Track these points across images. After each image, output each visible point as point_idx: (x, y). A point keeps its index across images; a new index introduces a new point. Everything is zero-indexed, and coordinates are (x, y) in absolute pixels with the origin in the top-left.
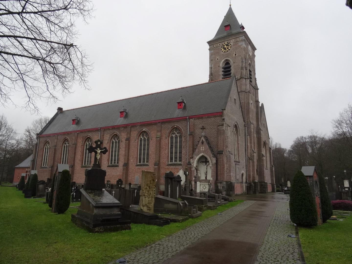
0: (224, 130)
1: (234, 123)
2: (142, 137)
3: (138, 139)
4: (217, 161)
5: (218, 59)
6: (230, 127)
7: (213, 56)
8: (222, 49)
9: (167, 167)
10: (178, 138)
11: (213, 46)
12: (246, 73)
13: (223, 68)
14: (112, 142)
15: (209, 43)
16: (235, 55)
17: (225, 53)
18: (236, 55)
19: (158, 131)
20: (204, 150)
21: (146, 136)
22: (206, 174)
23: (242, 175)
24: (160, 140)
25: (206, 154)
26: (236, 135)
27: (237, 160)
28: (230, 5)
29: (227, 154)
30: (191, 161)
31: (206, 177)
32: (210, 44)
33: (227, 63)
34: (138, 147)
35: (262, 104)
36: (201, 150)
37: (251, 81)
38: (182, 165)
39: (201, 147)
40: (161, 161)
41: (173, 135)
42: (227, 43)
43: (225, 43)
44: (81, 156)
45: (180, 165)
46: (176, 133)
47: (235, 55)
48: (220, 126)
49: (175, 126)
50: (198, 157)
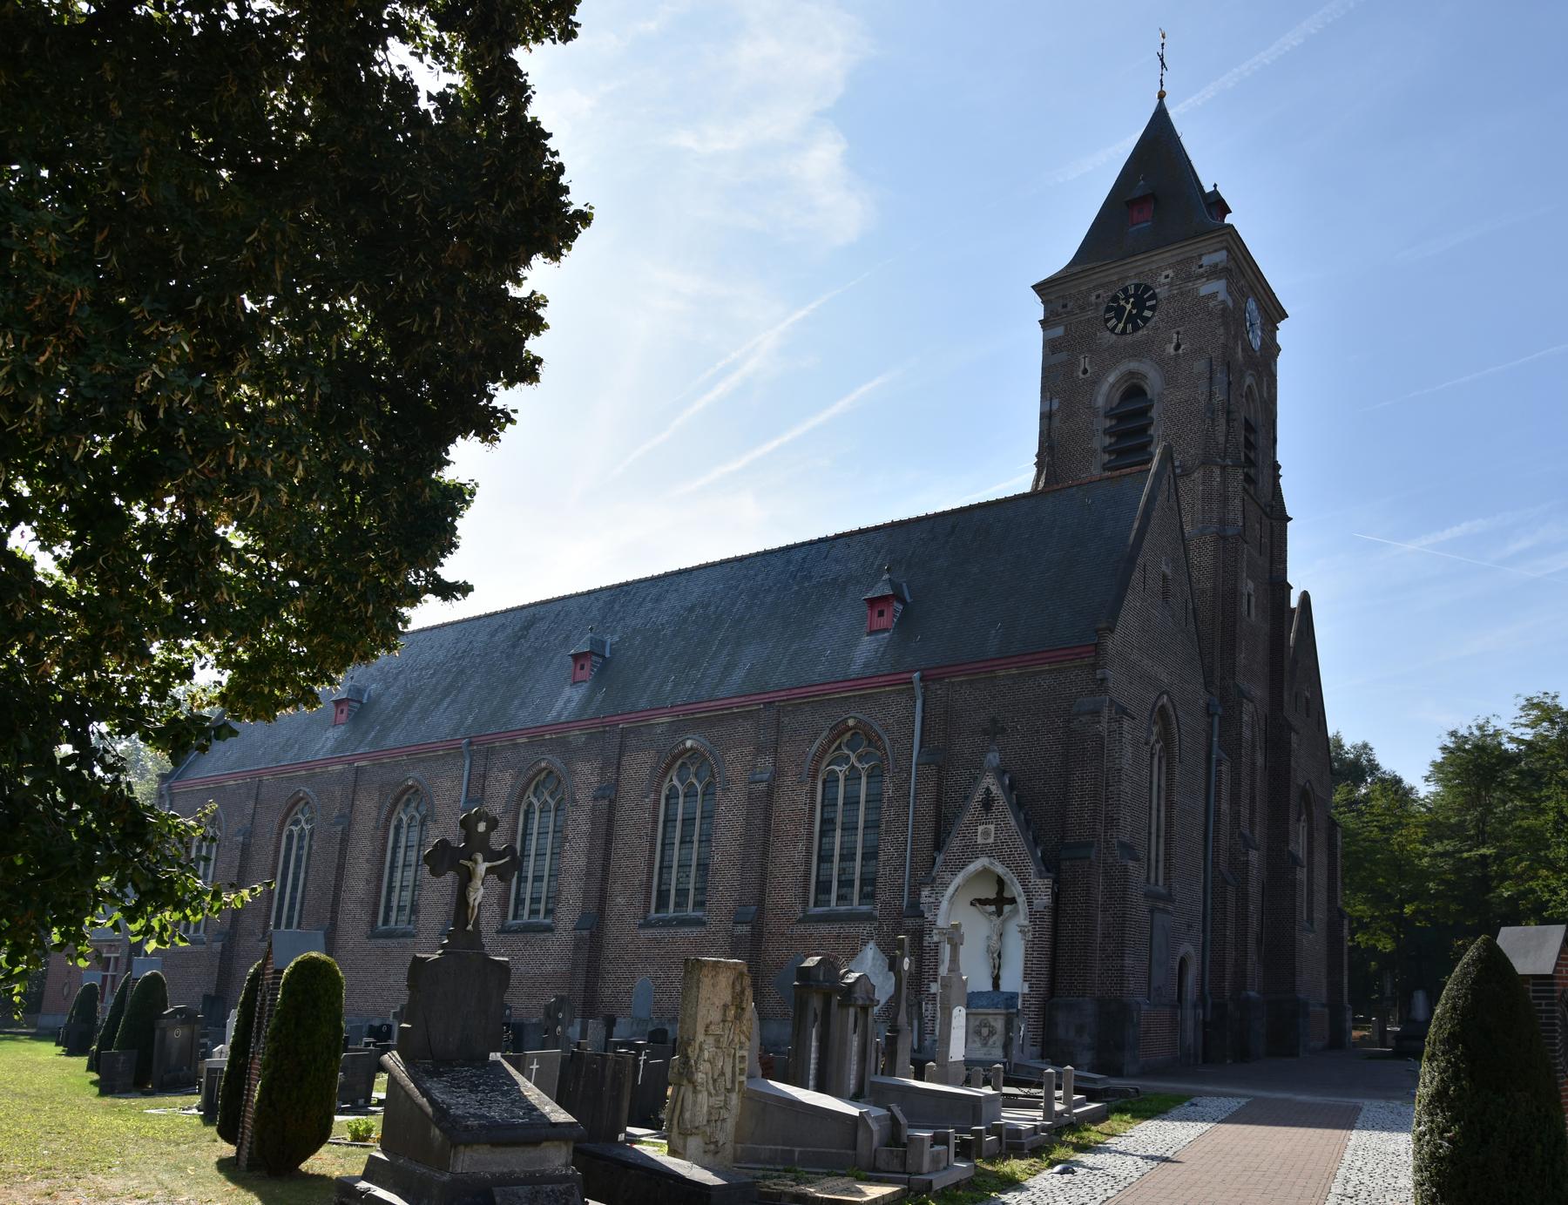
0: (1103, 738)
1: (1153, 697)
2: (676, 782)
3: (658, 792)
4: (1056, 897)
5: (1085, 371)
6: (1134, 718)
7: (1063, 356)
10: (864, 780)
12: (1227, 441)
13: (1108, 415)
14: (523, 807)
15: (1040, 288)
16: (1177, 347)
18: (1183, 347)
19: (759, 750)
20: (991, 840)
21: (696, 775)
22: (997, 960)
23: (1183, 962)
24: (770, 793)
25: (1003, 862)
26: (1160, 762)
27: (1161, 889)
29: (1110, 860)
30: (923, 900)
31: (996, 980)
32: (1043, 292)
33: (1134, 391)
34: (655, 830)
35: (1305, 597)
36: (980, 841)
37: (1248, 479)
39: (980, 828)
40: (769, 903)
41: (837, 768)
44: (368, 882)
45: (869, 917)
46: (853, 759)
49: (851, 722)
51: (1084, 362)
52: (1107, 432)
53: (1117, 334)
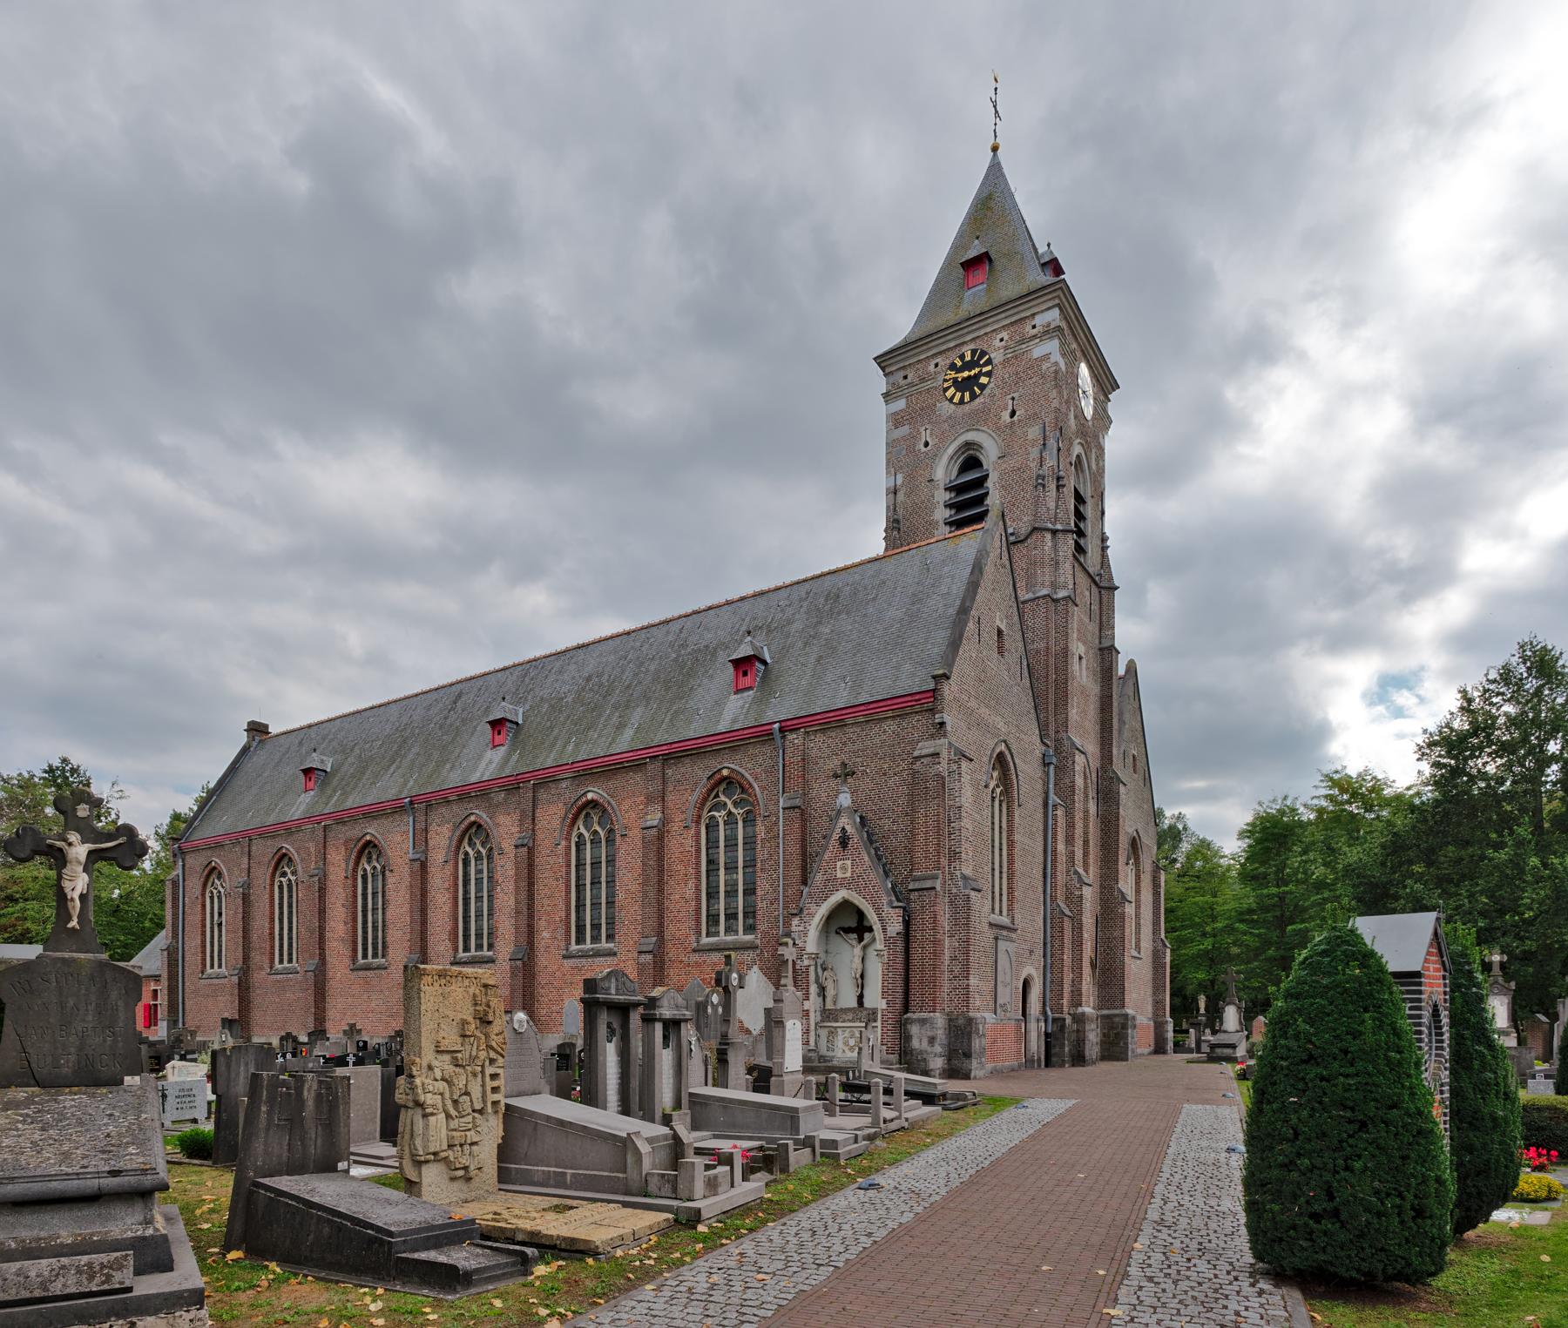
5: (926, 444)
7: (905, 430)
11: (905, 377)
16: (1013, 414)
47: (1013, 414)
51: (925, 435)
52: (949, 506)
53: (955, 404)
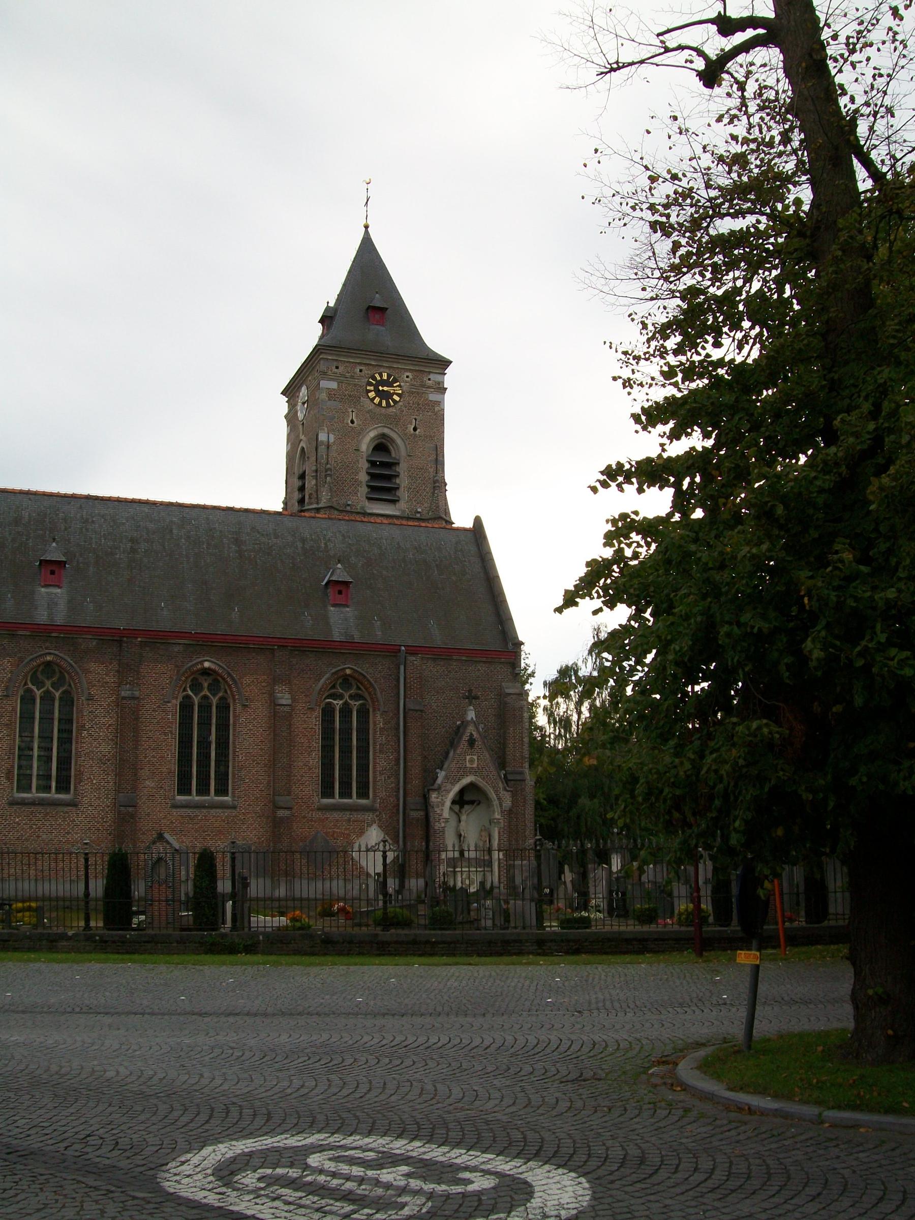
8: (371, 391)
9: (319, 815)
16: (415, 429)
17: (378, 410)
20: (475, 765)
25: (483, 779)
28: (366, 227)
33: (382, 446)
36: (468, 765)
38: (376, 810)
39: (468, 757)
42: (389, 376)
43: (381, 376)
48: (514, 697)
49: (348, 672)
50: (457, 788)
